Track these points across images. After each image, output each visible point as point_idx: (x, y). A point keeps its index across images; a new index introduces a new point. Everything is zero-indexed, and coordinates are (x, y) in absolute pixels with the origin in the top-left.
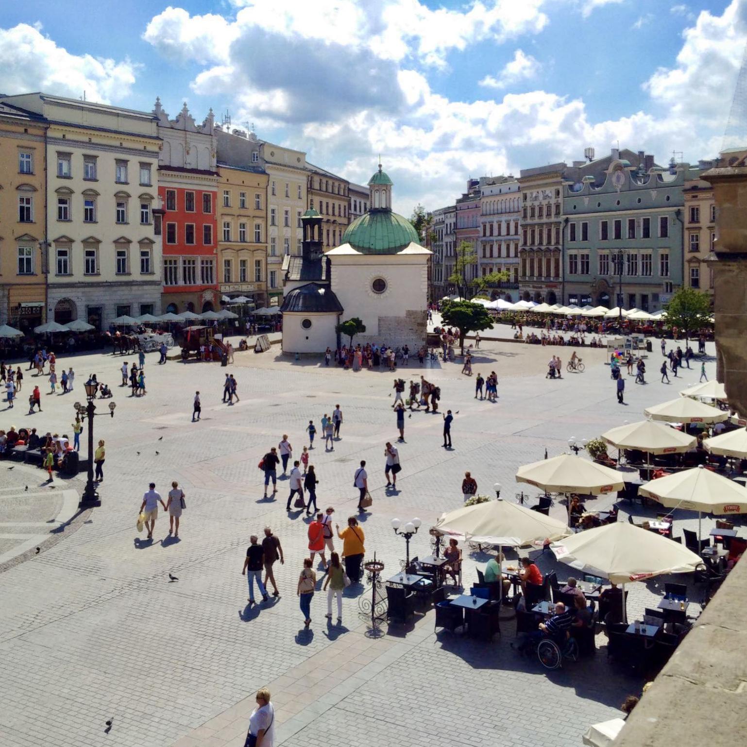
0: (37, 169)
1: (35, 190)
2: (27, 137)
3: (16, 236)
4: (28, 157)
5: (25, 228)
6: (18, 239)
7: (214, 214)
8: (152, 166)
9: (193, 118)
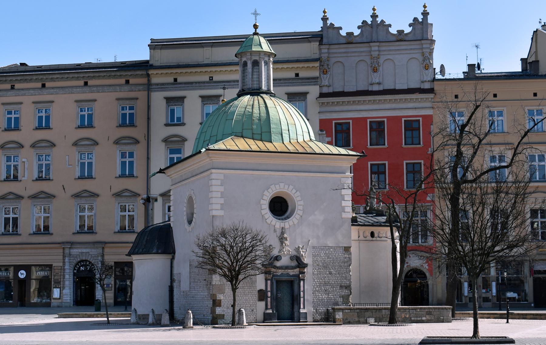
0: (140, 121)
1: (137, 142)
2: (127, 88)
3: (115, 190)
4: (131, 108)
5: (128, 184)
6: (118, 195)
7: (427, 144)
8: (308, 96)
9: (387, 23)
